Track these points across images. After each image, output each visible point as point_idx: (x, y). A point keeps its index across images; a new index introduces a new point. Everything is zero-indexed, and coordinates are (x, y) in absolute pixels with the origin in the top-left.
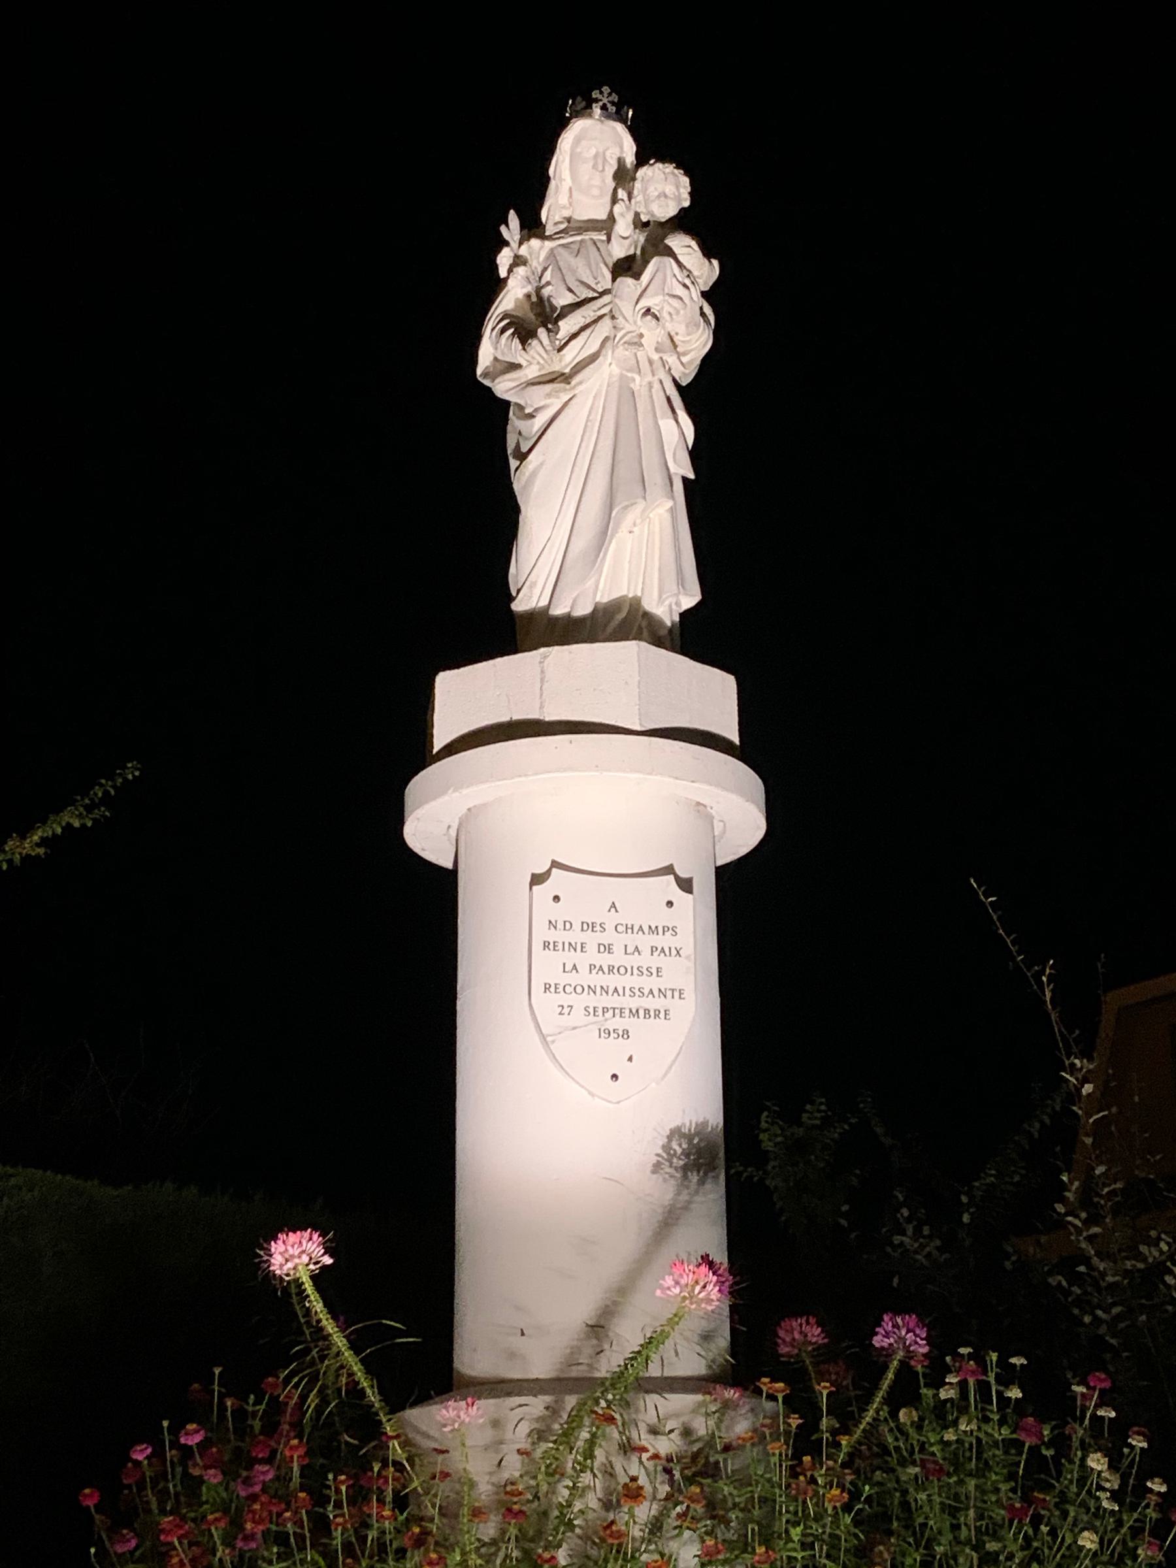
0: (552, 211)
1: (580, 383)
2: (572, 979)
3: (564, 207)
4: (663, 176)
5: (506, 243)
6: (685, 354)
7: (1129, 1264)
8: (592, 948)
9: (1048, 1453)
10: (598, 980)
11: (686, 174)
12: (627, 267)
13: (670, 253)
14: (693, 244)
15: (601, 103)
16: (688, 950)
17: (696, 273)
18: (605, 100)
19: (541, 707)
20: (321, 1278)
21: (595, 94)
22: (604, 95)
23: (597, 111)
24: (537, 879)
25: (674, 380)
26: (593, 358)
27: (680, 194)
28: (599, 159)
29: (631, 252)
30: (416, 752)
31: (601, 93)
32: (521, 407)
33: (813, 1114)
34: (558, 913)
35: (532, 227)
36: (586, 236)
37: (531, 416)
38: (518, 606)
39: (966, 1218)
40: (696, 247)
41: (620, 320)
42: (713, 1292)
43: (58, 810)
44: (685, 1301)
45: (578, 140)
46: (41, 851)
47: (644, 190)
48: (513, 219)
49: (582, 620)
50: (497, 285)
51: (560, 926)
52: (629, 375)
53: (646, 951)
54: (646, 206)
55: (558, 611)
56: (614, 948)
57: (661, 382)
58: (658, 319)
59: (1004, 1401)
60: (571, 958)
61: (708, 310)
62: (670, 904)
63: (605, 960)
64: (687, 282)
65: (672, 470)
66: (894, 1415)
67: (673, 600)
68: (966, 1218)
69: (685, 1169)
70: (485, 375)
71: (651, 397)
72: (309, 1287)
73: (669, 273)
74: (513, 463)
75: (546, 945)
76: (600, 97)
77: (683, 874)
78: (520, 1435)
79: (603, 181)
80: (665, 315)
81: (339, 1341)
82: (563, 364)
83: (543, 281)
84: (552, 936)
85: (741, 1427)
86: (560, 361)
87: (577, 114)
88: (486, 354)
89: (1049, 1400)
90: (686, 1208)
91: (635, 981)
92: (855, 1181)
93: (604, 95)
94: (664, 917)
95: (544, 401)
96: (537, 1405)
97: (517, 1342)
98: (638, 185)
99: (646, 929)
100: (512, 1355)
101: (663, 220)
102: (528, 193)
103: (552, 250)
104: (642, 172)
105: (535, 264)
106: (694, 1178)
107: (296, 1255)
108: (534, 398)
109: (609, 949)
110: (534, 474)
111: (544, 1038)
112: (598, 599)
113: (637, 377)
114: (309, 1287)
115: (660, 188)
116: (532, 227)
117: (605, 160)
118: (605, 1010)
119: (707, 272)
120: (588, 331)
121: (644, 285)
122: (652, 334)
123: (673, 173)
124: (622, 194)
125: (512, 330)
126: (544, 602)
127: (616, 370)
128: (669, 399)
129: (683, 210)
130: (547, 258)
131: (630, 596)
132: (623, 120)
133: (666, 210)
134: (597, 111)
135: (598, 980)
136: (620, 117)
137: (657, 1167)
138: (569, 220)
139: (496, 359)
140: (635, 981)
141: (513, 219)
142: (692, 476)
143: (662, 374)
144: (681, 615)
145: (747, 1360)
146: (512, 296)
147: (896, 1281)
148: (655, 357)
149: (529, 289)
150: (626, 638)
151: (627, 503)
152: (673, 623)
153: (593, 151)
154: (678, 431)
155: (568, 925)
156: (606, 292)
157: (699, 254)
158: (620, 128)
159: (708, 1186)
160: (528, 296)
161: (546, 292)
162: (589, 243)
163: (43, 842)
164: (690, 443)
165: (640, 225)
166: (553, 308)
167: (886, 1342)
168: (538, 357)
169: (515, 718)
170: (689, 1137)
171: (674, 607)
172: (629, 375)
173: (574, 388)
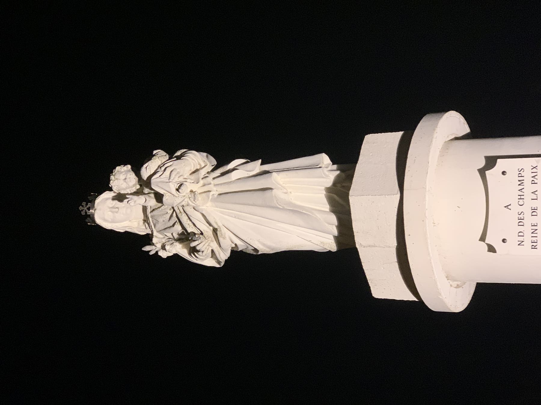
0: (141, 230)
1: (216, 223)
3: (139, 224)
4: (116, 181)
5: (157, 252)
6: (200, 164)
11: (115, 168)
12: (159, 197)
14: (145, 166)
15: (87, 211)
17: (160, 163)
18: (85, 208)
19: (389, 247)
22: (83, 208)
24: (491, 249)
25: (213, 170)
26: (203, 215)
27: (125, 171)
29: (152, 195)
30: (418, 307)
31: (82, 210)
34: (513, 240)
35: (148, 239)
36: (149, 215)
37: (236, 245)
38: (333, 247)
40: (146, 165)
41: (183, 203)
47: (124, 189)
48: (147, 248)
49: (339, 219)
50: (176, 257)
51: (521, 239)
52: (211, 197)
54: (132, 187)
55: (336, 232)
56: (534, 206)
57: (214, 178)
58: (181, 185)
61: (178, 153)
62: (504, 173)
64: (163, 168)
67: (325, 170)
70: (219, 262)
71: (221, 184)
73: (158, 180)
74: (259, 253)
76: (84, 211)
77: (482, 163)
79: (124, 207)
80: (181, 179)
82: (208, 230)
83: (172, 237)
84: (528, 244)
86: (207, 232)
87: (94, 221)
88: (210, 262)
93: (83, 208)
94: (512, 177)
98: (122, 192)
99: (521, 187)
101: (137, 179)
102: (135, 242)
103: (158, 232)
105: (164, 241)
110: (264, 245)
112: (328, 210)
113: (211, 193)
115: (122, 182)
116: (148, 239)
117: (113, 208)
120: (191, 217)
121: (165, 192)
123: (114, 176)
125: (196, 254)
126: (332, 238)
127: (209, 204)
128: (223, 174)
129: (133, 169)
130: (162, 234)
131: (325, 193)
133: (132, 178)
136: (93, 201)
139: (212, 257)
141: (147, 248)
142: (260, 161)
144: (333, 164)
148: (202, 182)
151: (275, 202)
152: (337, 170)
153: (110, 213)
155: (521, 234)
157: (150, 162)
158: (98, 201)
160: (180, 243)
161: (176, 236)
162: (152, 214)
164: (243, 161)
166: (182, 234)
168: (205, 246)
169: (396, 261)
171: (329, 168)
172: (211, 197)
173: (219, 226)
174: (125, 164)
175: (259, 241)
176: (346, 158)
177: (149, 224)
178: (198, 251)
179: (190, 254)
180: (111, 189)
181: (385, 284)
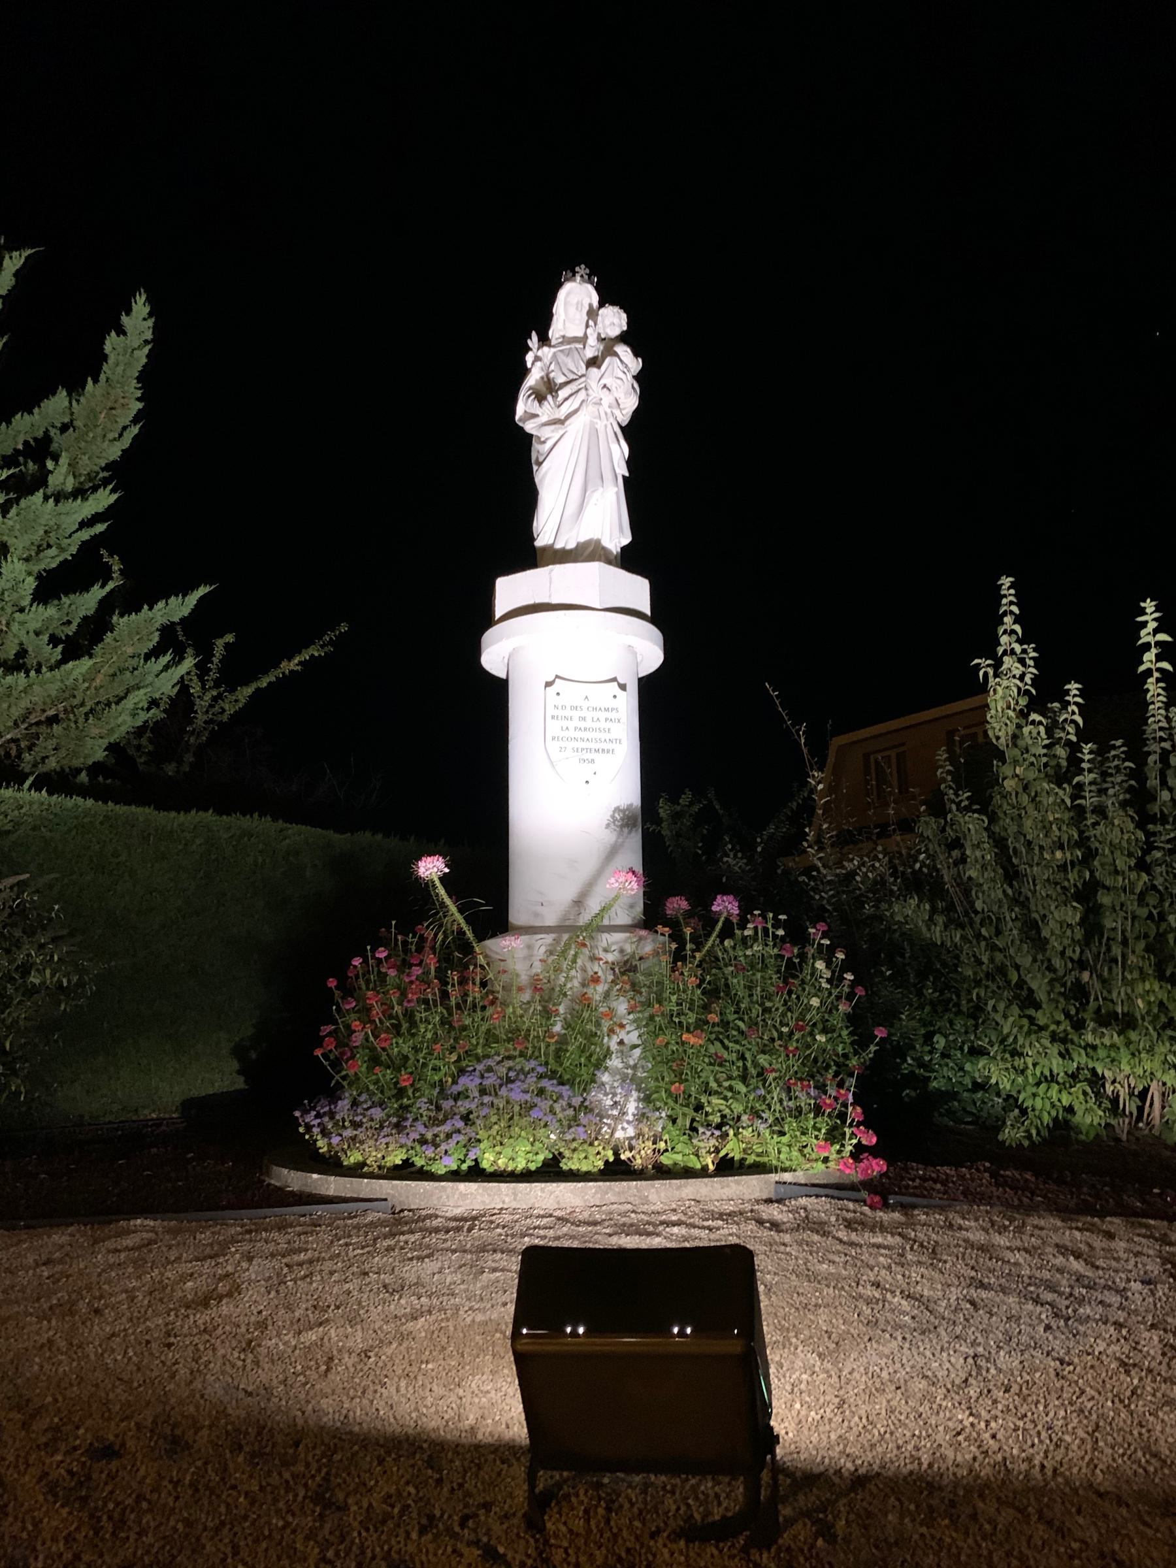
2: (566, 734)
5: (530, 349)
7: (838, 871)
8: (576, 718)
9: (797, 961)
10: (579, 734)
12: (593, 362)
13: (616, 354)
14: (629, 350)
16: (624, 720)
20: (444, 879)
21: (577, 269)
22: (582, 270)
23: (578, 278)
24: (548, 684)
26: (576, 411)
28: (579, 305)
30: (486, 619)
32: (539, 438)
33: (684, 800)
34: (559, 701)
36: (572, 346)
37: (544, 442)
38: (539, 543)
39: (759, 849)
41: (590, 392)
42: (635, 885)
43: (307, 647)
44: (623, 889)
45: (568, 294)
46: (299, 668)
49: (570, 551)
50: (524, 372)
53: (603, 720)
55: (558, 546)
59: (775, 936)
60: (565, 723)
61: (636, 386)
63: (582, 725)
65: (618, 471)
66: (722, 942)
68: (759, 849)
69: (622, 827)
70: (520, 420)
72: (438, 883)
74: (535, 468)
75: (553, 717)
77: (622, 682)
78: (541, 952)
80: (613, 389)
81: (453, 908)
85: (648, 948)
87: (567, 280)
88: (521, 409)
89: (797, 936)
90: (622, 845)
91: (597, 735)
92: (705, 832)
93: (582, 270)
95: (549, 434)
96: (549, 938)
97: (539, 909)
98: (599, 318)
100: (537, 915)
102: (542, 322)
104: (602, 311)
106: (626, 830)
107: (431, 868)
108: (545, 433)
109: (584, 719)
110: (546, 473)
111: (552, 763)
114: (438, 883)
116: (544, 340)
118: (582, 749)
119: (635, 365)
122: (607, 399)
124: (591, 323)
126: (551, 542)
132: (592, 283)
133: (615, 332)
134: (578, 278)
135: (579, 734)
136: (590, 282)
137: (608, 826)
138: (563, 337)
140: (597, 735)
142: (627, 474)
143: (612, 420)
145: (652, 916)
146: (533, 378)
147: (724, 880)
148: (609, 411)
149: (543, 374)
150: (593, 560)
154: (620, 451)
156: (583, 376)
159: (633, 834)
160: (542, 378)
161: (552, 375)
163: (300, 663)
165: (601, 339)
167: (718, 909)
170: (623, 811)
174: (628, 324)
175: (549, 469)
176: (629, 560)
177: (562, 343)
178: (540, 402)
179: (530, 388)
180: (602, 304)
181: (510, 590)
